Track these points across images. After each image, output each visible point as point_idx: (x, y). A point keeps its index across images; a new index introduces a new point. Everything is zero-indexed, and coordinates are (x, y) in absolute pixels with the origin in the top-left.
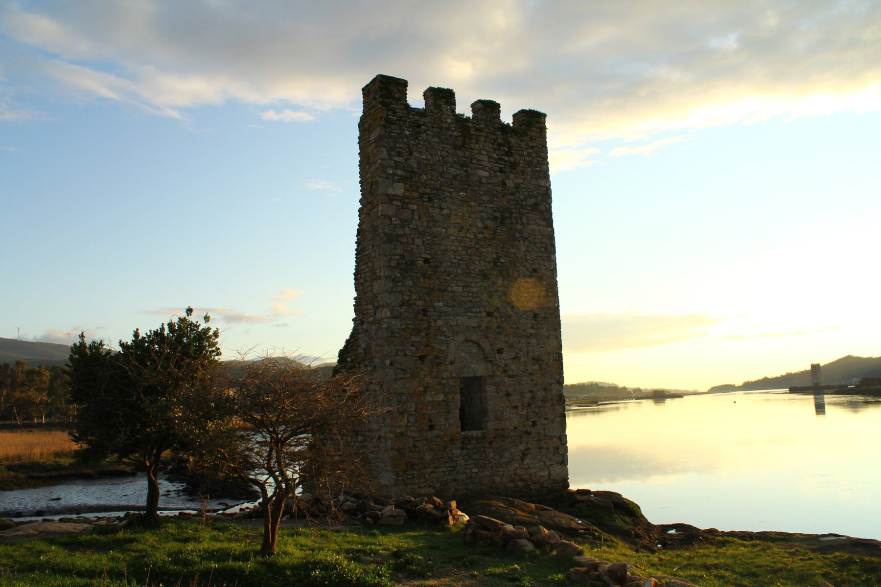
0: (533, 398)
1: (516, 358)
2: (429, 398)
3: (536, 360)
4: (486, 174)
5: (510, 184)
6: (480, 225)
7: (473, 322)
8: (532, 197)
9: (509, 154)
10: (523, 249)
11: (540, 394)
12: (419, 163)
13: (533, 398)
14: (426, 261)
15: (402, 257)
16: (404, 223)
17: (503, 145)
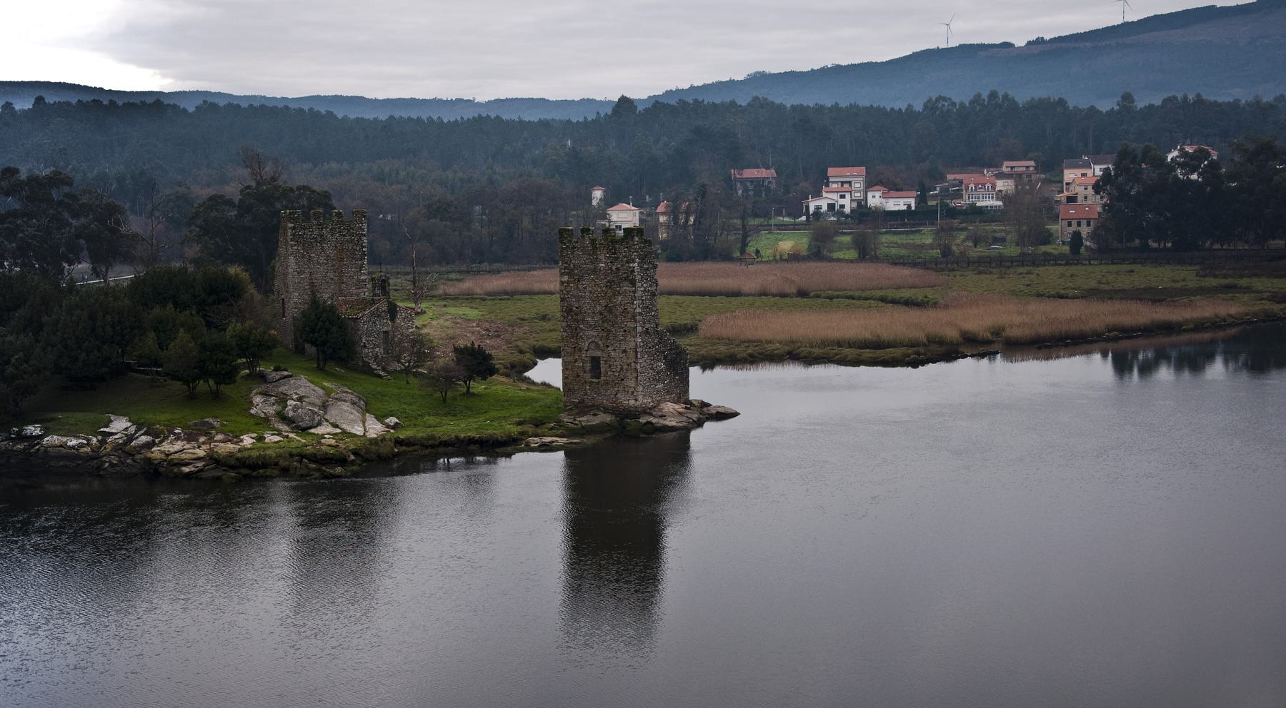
0: (622, 368)
1: (614, 350)
2: (577, 364)
3: (624, 351)
4: (604, 265)
5: (614, 268)
6: (599, 290)
7: (596, 334)
8: (625, 273)
9: (615, 253)
10: (620, 299)
11: (625, 367)
12: (574, 265)
13: (622, 368)
14: (577, 308)
15: (567, 307)
16: (568, 292)
17: (612, 249)
